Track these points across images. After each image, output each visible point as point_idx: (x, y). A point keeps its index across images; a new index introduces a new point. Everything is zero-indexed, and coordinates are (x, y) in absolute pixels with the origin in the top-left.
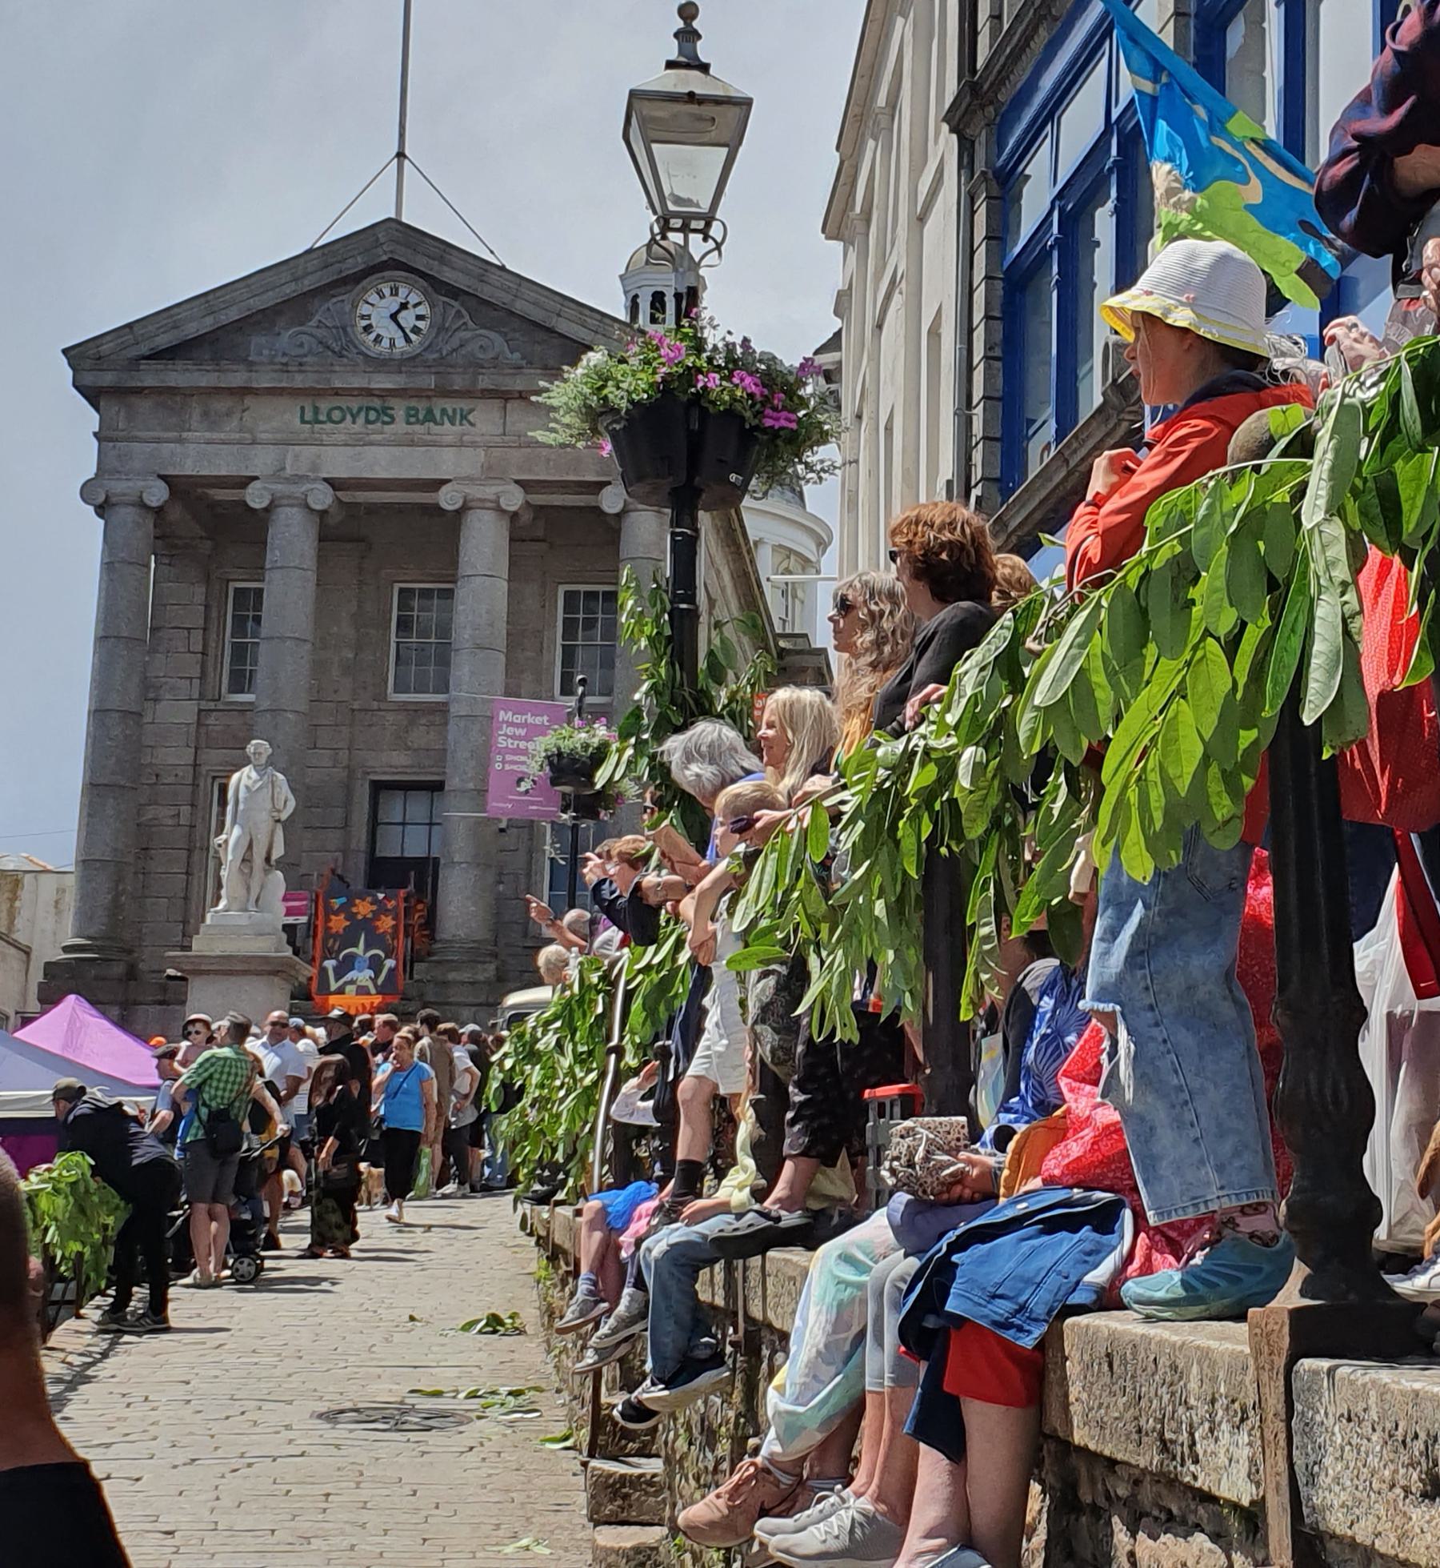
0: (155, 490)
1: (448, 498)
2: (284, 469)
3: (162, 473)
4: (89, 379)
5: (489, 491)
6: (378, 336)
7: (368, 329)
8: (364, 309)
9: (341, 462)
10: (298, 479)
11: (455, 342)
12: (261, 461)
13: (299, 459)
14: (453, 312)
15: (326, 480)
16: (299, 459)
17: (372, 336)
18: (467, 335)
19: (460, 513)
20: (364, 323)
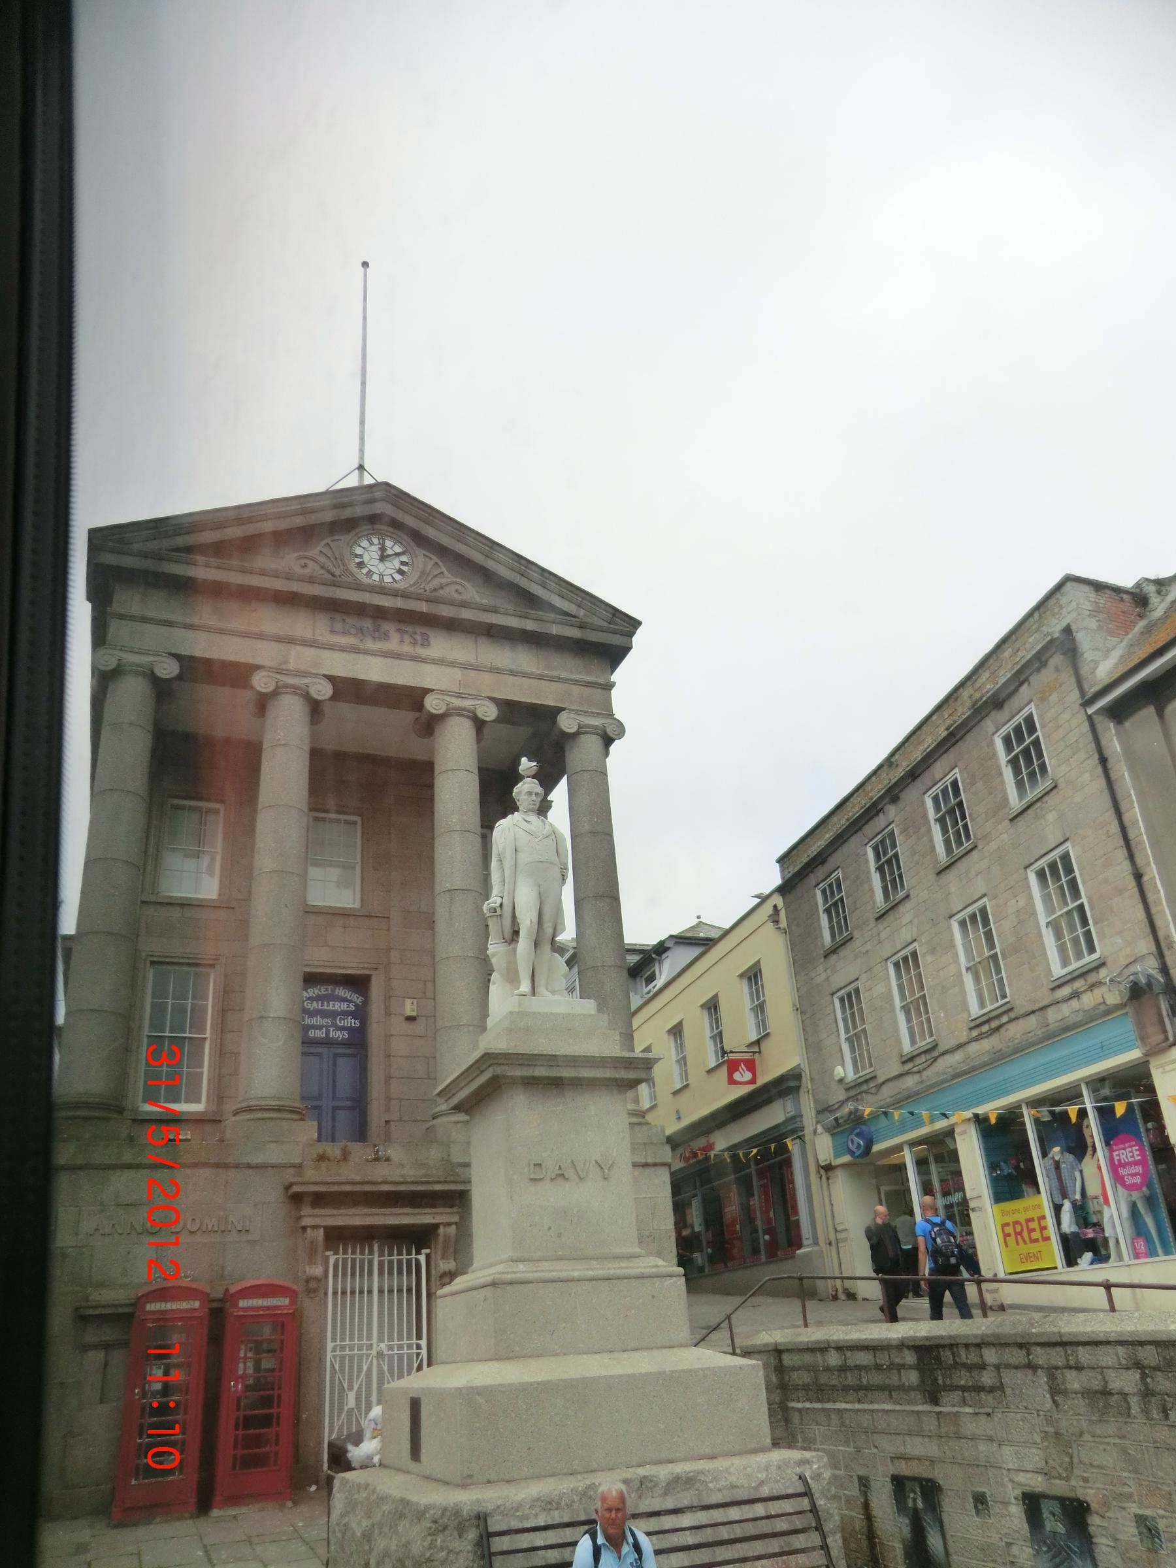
0: (166, 666)
1: (432, 704)
2: (287, 662)
3: (173, 651)
4: (109, 559)
5: (466, 703)
6: (370, 571)
7: (361, 565)
8: (359, 551)
9: (342, 665)
10: (299, 674)
11: (436, 583)
12: (263, 653)
13: (299, 658)
14: (432, 563)
15: (325, 676)
16: (299, 658)
17: (365, 571)
18: (444, 581)
19: (442, 717)
20: (357, 560)
